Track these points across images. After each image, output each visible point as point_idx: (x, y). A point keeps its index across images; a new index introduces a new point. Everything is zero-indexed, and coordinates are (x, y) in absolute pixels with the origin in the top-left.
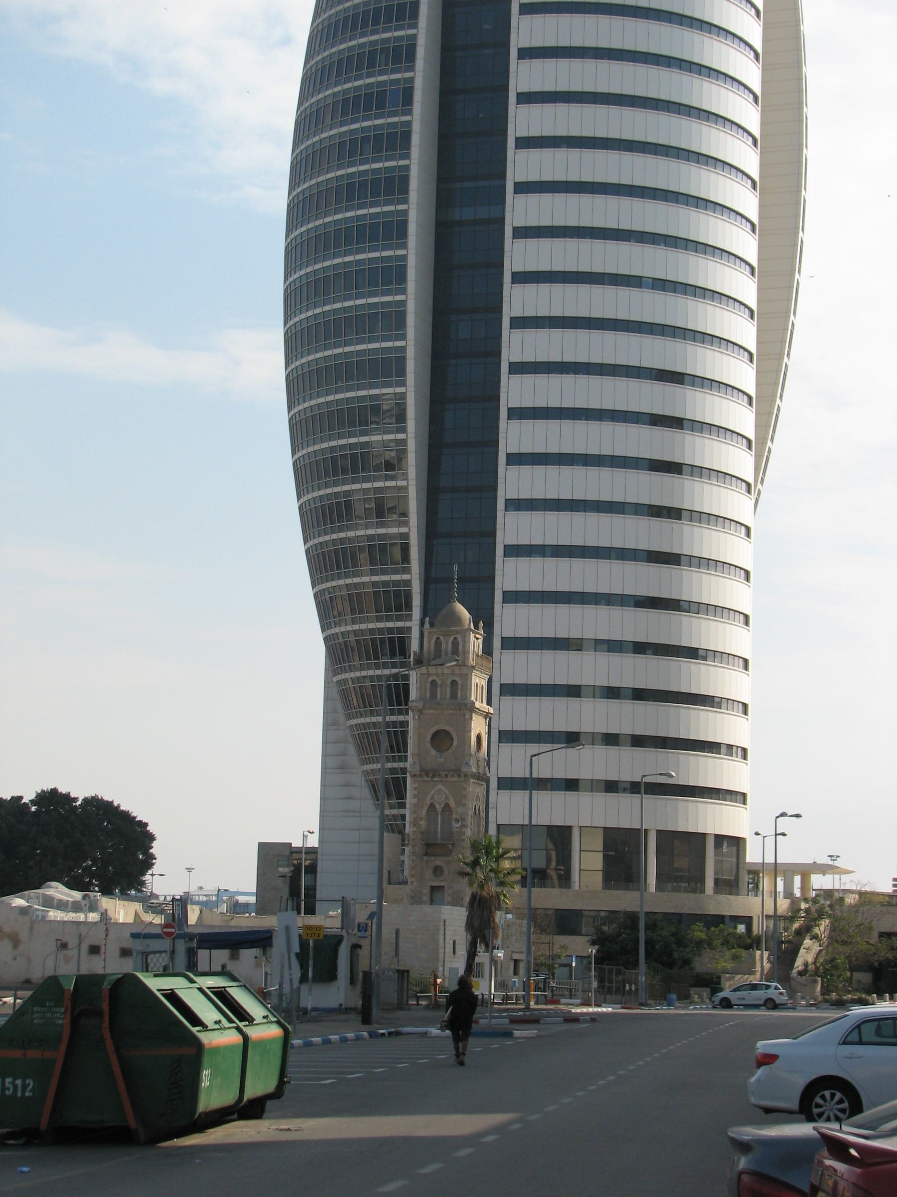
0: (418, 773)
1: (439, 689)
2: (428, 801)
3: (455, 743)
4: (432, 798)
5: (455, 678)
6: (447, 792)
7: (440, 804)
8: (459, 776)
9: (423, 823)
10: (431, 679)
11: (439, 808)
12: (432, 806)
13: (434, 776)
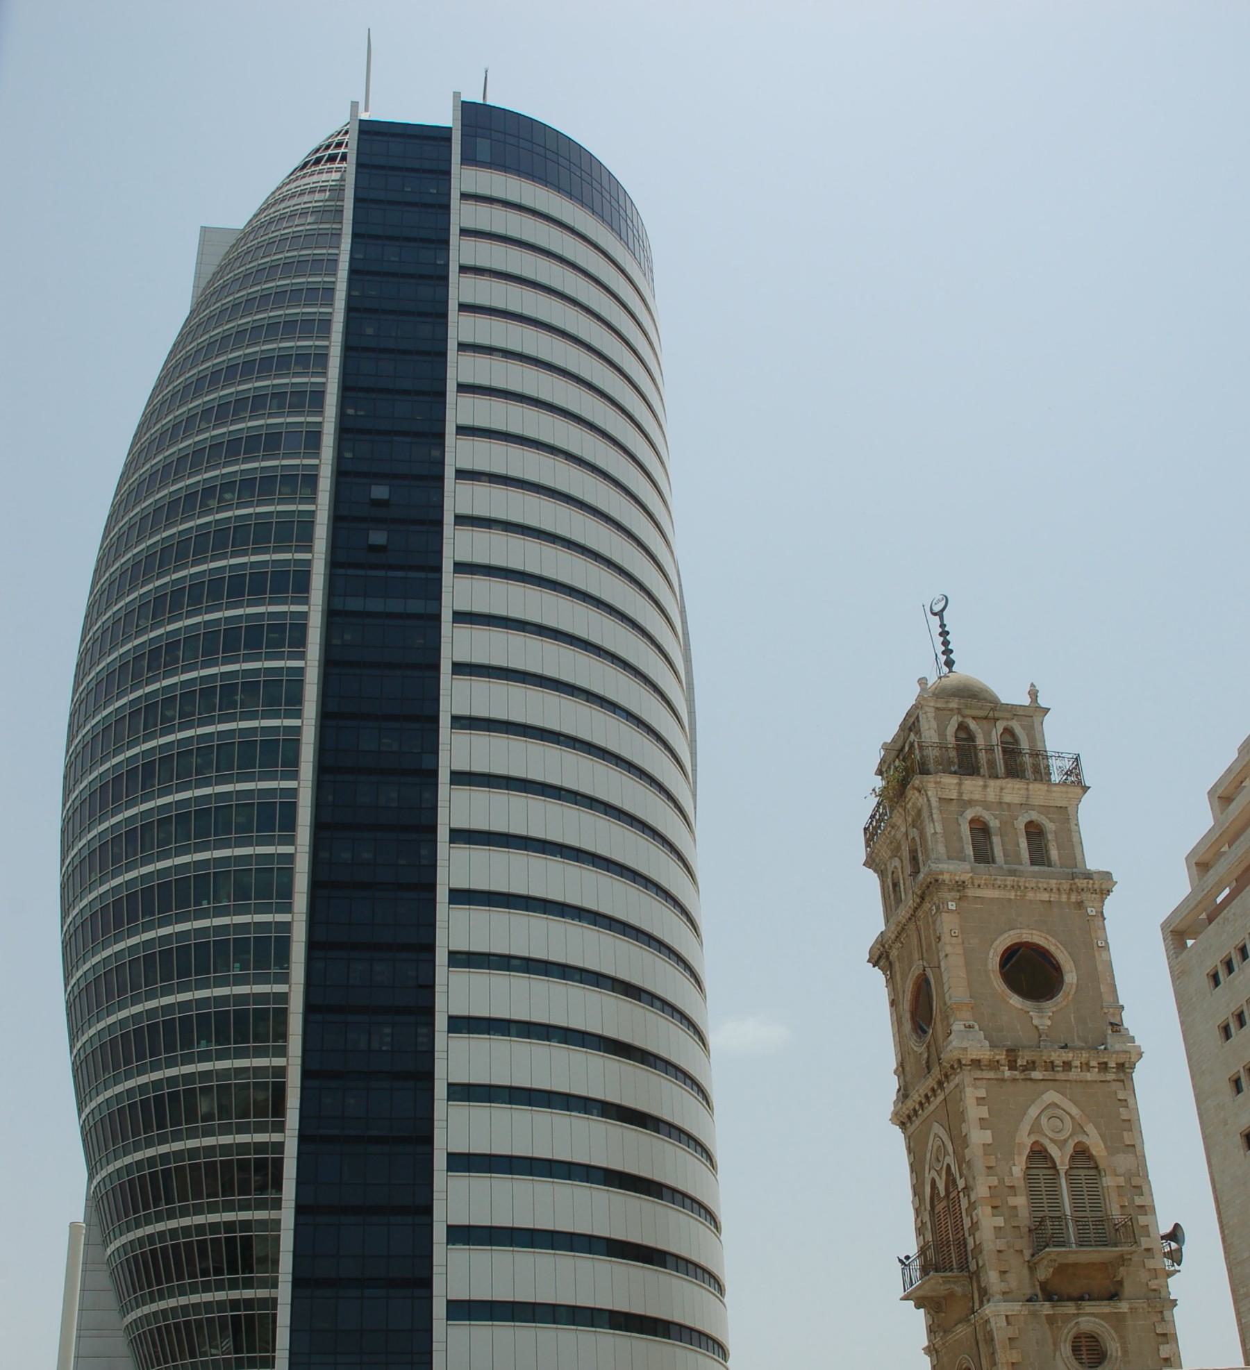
1: (996, 840)
2: (1025, 1140)
4: (1035, 1128)
6: (1074, 1111)
7: (1061, 1144)
8: (1104, 1067)
9: (1020, 1201)
10: (970, 814)
11: (1061, 1157)
12: (1039, 1154)
13: (1032, 1066)
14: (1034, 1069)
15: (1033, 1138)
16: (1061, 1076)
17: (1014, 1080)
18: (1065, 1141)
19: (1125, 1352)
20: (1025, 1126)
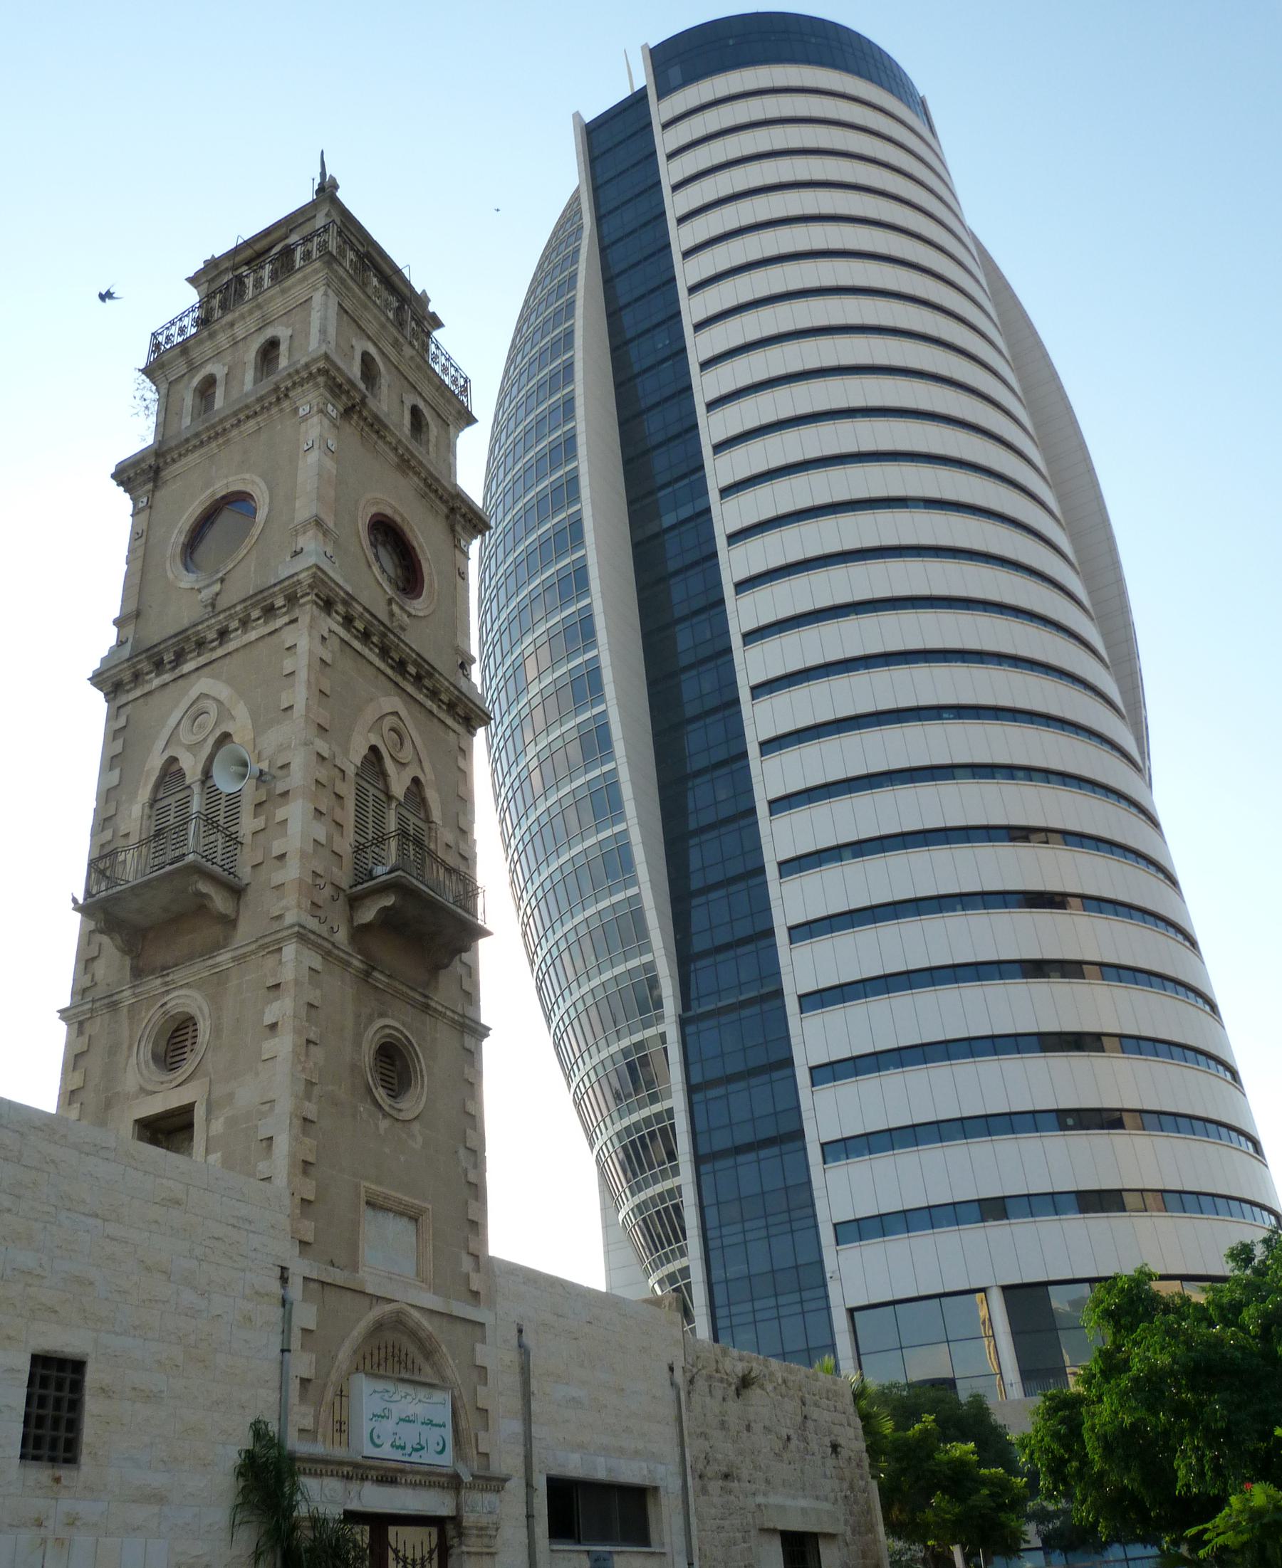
0: (127, 676)
2: (156, 762)
3: (261, 515)
5: (269, 333)
7: (192, 748)
11: (191, 766)
13: (180, 658)
14: (186, 662)
15: (166, 756)
16: (220, 652)
17: (165, 685)
18: (205, 740)
19: (216, 1030)
20: (161, 743)
